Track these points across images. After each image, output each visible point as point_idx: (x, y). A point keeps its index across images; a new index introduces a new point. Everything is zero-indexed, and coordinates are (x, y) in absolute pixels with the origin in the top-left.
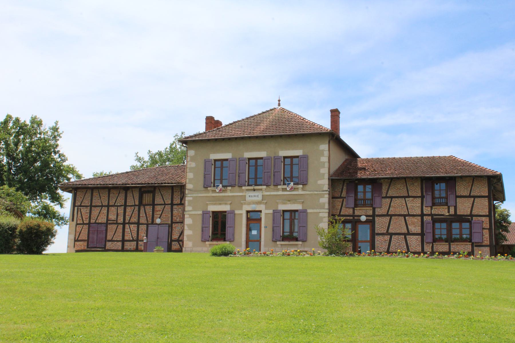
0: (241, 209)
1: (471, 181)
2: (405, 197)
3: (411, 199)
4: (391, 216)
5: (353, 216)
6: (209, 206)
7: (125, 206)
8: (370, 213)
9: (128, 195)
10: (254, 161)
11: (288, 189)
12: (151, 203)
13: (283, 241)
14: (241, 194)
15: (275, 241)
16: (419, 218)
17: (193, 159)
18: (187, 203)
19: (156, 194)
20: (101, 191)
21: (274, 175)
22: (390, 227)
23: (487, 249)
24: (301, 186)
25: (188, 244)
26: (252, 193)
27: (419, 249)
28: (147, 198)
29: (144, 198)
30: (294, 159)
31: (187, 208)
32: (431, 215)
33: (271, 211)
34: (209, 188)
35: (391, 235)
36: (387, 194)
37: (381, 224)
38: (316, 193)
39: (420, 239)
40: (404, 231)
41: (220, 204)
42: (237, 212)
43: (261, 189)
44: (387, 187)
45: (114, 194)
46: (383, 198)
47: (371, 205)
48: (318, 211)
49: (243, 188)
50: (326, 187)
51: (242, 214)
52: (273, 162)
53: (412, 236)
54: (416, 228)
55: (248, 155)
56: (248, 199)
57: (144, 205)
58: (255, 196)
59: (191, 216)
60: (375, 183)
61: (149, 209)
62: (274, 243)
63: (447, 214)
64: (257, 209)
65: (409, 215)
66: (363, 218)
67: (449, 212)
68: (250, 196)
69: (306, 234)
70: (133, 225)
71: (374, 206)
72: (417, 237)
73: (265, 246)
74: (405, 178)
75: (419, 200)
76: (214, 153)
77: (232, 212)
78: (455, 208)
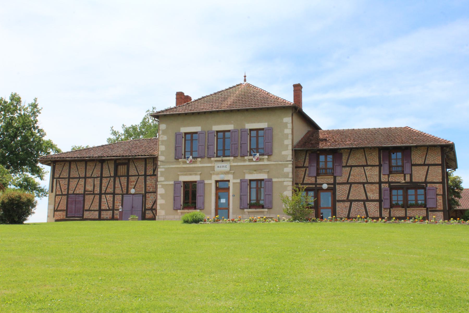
1: (426, 150)
2: (364, 166)
3: (369, 167)
4: (351, 184)
5: (316, 184)
6: (180, 177)
7: (102, 177)
8: (332, 181)
9: (104, 167)
10: (222, 133)
11: (254, 160)
12: (126, 174)
13: (250, 208)
15: (242, 208)
16: (378, 185)
17: (164, 132)
18: (159, 174)
19: (131, 166)
20: (79, 164)
21: (241, 147)
22: (350, 195)
23: (441, 214)
24: (266, 157)
25: (160, 212)
26: (220, 164)
27: (377, 214)
28: (122, 170)
29: (119, 170)
30: (226, 133)
31: (160, 179)
32: (389, 183)
33: (238, 181)
34: (180, 160)
35: (351, 201)
36: (347, 163)
37: (341, 192)
38: (280, 163)
39: (378, 205)
40: (364, 197)
41: (191, 175)
42: (206, 182)
43: (229, 160)
44: (347, 157)
45: (90, 166)
46: (343, 167)
47: (333, 174)
48: (282, 180)
49: (212, 159)
50: (290, 158)
51: (211, 184)
52: (206, 136)
53: (370, 203)
55: (216, 128)
56: (217, 169)
57: (119, 177)
58: (223, 167)
59: (163, 186)
60: (336, 153)
61: (124, 180)
62: (241, 210)
63: (404, 181)
64: (226, 179)
65: (368, 183)
66: (325, 186)
67: (405, 179)
68: (218, 167)
69: (271, 202)
70: (108, 196)
71: (335, 175)
72: (376, 203)
73: (233, 213)
74: (363, 148)
75: (377, 168)
76: (185, 126)
77: (202, 182)
78: (411, 175)
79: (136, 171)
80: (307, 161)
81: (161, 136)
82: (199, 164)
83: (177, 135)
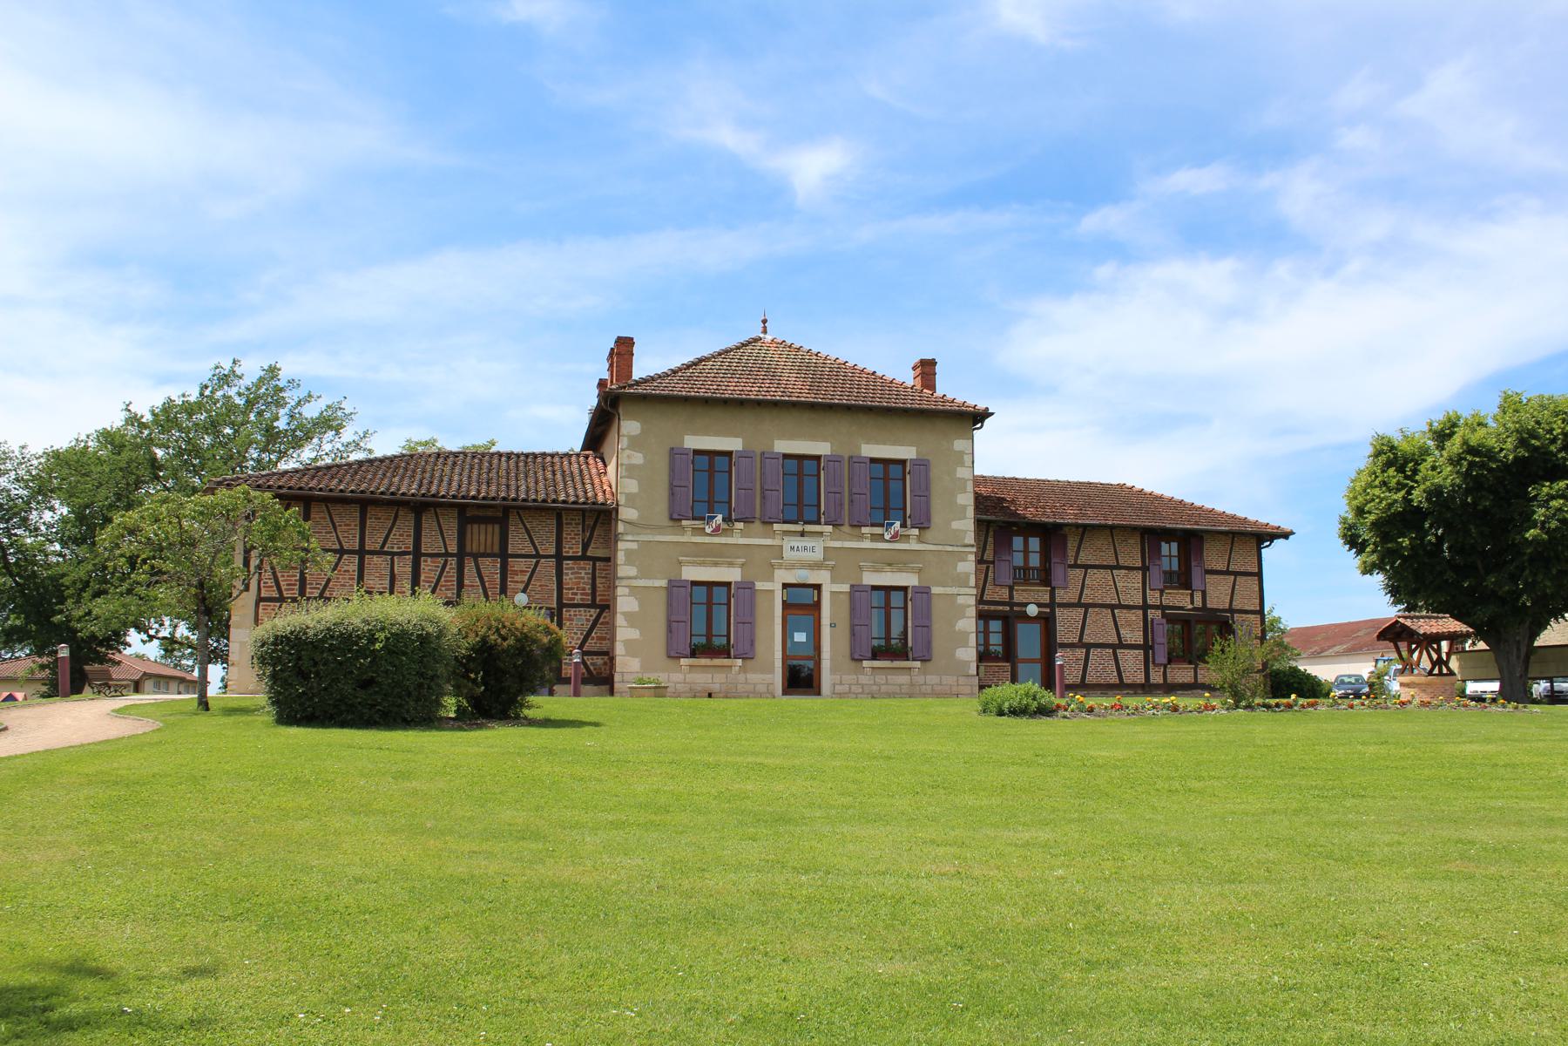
0: (771, 578)
4: (1087, 606)
5: (1011, 604)
7: (417, 555)
8: (1046, 598)
11: (887, 537)
12: (496, 549)
14: (769, 542)
15: (857, 659)
17: (635, 443)
18: (621, 557)
20: (337, 510)
21: (851, 501)
24: (916, 532)
25: (627, 666)
27: (1140, 679)
28: (482, 536)
29: (475, 537)
31: (624, 570)
32: (1161, 607)
33: (846, 588)
34: (684, 523)
35: (1088, 647)
37: (1067, 624)
39: (1141, 657)
40: (1113, 639)
41: (716, 564)
42: (759, 586)
46: (1070, 566)
48: (954, 590)
51: (772, 591)
54: (1134, 635)
55: (783, 446)
56: (787, 554)
57: (476, 556)
59: (634, 591)
60: (1051, 535)
61: (491, 567)
62: (853, 664)
66: (1032, 610)
73: (833, 670)
74: (1112, 528)
77: (747, 586)
78: (1204, 593)
79: (528, 544)
80: (990, 547)
81: (628, 452)
82: (738, 537)
83: (675, 453)
